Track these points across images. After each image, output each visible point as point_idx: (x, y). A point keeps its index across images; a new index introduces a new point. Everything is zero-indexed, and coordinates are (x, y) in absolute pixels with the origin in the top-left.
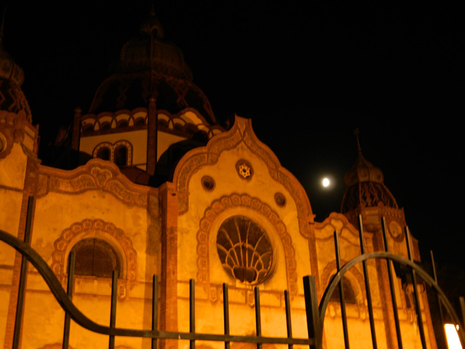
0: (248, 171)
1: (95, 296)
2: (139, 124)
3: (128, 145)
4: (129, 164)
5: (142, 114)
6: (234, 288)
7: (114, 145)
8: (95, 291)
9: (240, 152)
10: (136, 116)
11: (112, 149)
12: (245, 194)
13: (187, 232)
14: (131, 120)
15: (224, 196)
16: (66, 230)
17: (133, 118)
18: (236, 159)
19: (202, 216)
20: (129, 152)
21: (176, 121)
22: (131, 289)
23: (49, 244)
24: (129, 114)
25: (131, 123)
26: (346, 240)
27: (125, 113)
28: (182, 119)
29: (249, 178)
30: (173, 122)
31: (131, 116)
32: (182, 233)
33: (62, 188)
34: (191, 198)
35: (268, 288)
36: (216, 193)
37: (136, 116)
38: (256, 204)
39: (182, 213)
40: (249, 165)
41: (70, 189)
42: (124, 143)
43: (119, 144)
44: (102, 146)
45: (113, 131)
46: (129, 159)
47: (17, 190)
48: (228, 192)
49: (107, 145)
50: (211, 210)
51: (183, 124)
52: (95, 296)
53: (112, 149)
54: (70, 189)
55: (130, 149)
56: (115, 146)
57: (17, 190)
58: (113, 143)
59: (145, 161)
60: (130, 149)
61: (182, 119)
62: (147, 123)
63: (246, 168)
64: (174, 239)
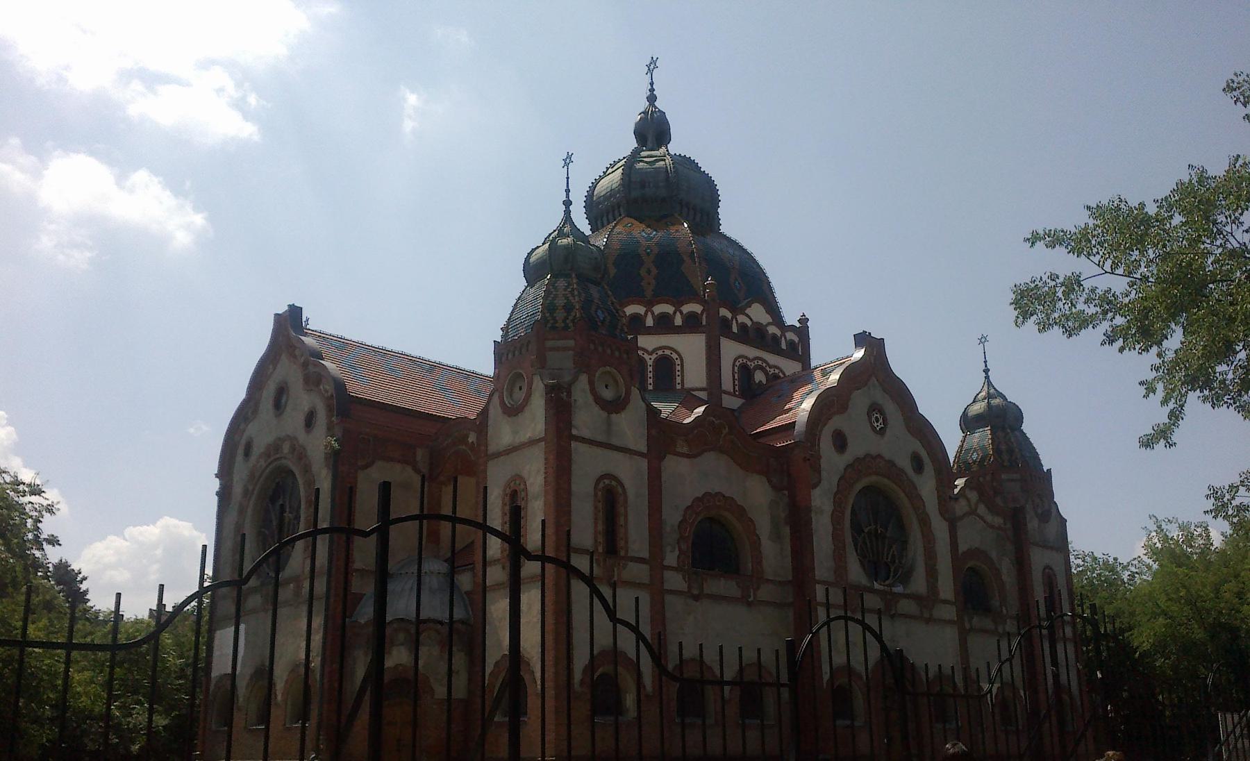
3: (675, 356)
4: (679, 387)
5: (697, 308)
6: (872, 590)
7: (651, 354)
10: (687, 308)
11: (650, 360)
12: (879, 456)
14: (678, 315)
15: (857, 460)
16: (688, 508)
17: (681, 313)
20: (679, 368)
22: (758, 588)
25: (678, 321)
26: (982, 518)
29: (882, 432)
31: (678, 310)
33: (679, 450)
34: (824, 464)
36: (848, 457)
37: (687, 308)
38: (891, 469)
39: (815, 486)
40: (881, 412)
41: (685, 450)
42: (667, 352)
43: (660, 352)
45: (649, 331)
46: (678, 380)
48: (861, 453)
50: (845, 481)
51: (749, 323)
53: (650, 360)
54: (685, 450)
55: (678, 362)
56: (654, 356)
58: (650, 349)
60: (678, 362)
64: (809, 522)
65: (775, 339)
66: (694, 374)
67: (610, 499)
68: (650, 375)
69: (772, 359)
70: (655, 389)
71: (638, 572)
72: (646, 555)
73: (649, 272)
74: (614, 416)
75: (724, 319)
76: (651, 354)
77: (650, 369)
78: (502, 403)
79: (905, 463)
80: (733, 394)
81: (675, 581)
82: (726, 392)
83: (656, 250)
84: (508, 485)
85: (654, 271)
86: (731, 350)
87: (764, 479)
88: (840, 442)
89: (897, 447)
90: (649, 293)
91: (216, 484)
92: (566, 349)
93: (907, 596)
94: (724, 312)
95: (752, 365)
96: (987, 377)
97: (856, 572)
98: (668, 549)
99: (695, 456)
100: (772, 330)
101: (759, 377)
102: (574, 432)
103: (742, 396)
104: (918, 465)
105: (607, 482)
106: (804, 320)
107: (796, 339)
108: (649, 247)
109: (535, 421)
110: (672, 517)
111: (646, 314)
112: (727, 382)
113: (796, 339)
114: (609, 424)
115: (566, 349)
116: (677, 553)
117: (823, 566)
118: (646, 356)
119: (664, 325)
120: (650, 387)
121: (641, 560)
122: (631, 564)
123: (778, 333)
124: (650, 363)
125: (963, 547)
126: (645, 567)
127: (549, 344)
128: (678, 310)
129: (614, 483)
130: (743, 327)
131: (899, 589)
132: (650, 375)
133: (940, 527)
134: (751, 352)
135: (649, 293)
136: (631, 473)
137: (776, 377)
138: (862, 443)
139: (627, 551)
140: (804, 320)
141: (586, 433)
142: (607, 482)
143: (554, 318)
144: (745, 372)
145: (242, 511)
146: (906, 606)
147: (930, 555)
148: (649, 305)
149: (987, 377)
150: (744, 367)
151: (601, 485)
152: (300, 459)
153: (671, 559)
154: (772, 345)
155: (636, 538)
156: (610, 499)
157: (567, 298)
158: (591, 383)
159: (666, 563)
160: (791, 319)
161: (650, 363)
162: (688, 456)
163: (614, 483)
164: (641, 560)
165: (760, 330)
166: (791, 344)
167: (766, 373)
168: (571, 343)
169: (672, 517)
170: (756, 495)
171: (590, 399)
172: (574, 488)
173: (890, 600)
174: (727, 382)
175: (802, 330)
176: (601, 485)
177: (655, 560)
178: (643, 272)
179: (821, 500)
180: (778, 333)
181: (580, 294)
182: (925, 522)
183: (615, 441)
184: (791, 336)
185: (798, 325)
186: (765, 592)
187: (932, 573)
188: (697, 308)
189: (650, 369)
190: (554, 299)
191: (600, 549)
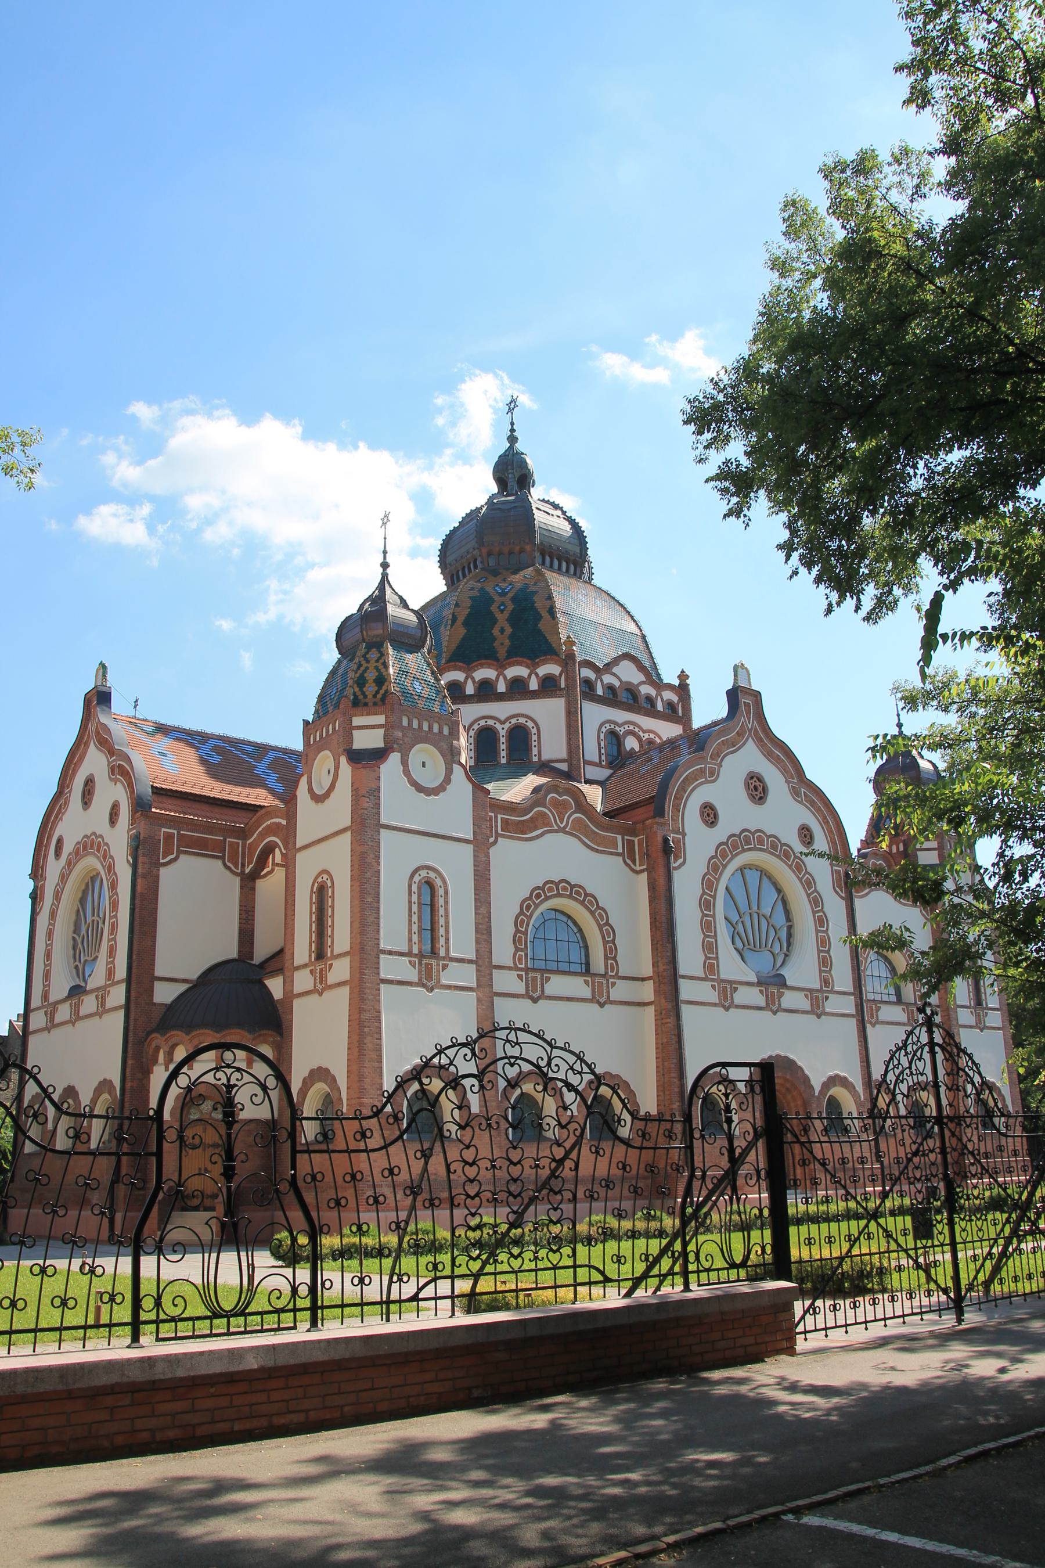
2: (549, 687)
3: (530, 724)
4: (535, 759)
5: (551, 669)
10: (543, 670)
11: (502, 730)
17: (537, 675)
20: (535, 737)
21: (608, 679)
24: (527, 667)
25: (534, 685)
27: (520, 664)
28: (614, 675)
30: (602, 681)
31: (533, 672)
37: (543, 670)
42: (522, 720)
43: (514, 721)
44: (482, 723)
45: (501, 697)
46: (535, 751)
49: (491, 722)
51: (617, 684)
53: (502, 730)
55: (534, 731)
56: (507, 726)
58: (502, 718)
59: (563, 754)
60: (534, 731)
61: (614, 675)
62: (563, 685)
63: (758, 783)
65: (649, 699)
66: (551, 745)
67: (428, 893)
68: (503, 747)
69: (646, 722)
70: (508, 763)
71: (468, 976)
73: (502, 631)
75: (588, 683)
76: (503, 723)
77: (503, 740)
80: (599, 765)
81: (507, 981)
82: (586, 762)
83: (511, 607)
85: (509, 630)
86: (595, 716)
88: (710, 815)
89: (782, 815)
90: (502, 652)
91: (30, 885)
92: (373, 727)
94: (587, 673)
95: (621, 730)
100: (646, 690)
101: (631, 744)
103: (610, 765)
104: (806, 834)
106: (683, 676)
107: (675, 698)
108: (503, 604)
109: (339, 809)
111: (498, 677)
112: (591, 747)
113: (675, 698)
115: (373, 727)
117: (689, 957)
118: (498, 726)
119: (518, 689)
120: (504, 761)
123: (653, 692)
124: (503, 733)
125: (864, 930)
127: (357, 721)
128: (533, 672)
129: (432, 875)
130: (611, 688)
132: (503, 747)
133: (834, 906)
134: (621, 716)
135: (502, 652)
137: (650, 742)
138: (738, 813)
139: (447, 950)
140: (683, 676)
143: (363, 693)
144: (615, 738)
145: (53, 915)
147: (823, 943)
148: (501, 667)
150: (613, 733)
152: (105, 858)
154: (647, 707)
155: (460, 938)
156: (428, 893)
157: (377, 668)
158: (405, 763)
160: (670, 677)
161: (503, 733)
165: (631, 690)
166: (670, 705)
167: (639, 739)
168: (380, 719)
170: (611, 880)
174: (591, 747)
175: (683, 689)
176: (417, 878)
178: (496, 631)
179: (686, 884)
180: (653, 692)
182: (816, 902)
184: (668, 695)
185: (677, 682)
186: (620, 990)
187: (825, 962)
188: (551, 669)
189: (503, 740)
190: (365, 671)
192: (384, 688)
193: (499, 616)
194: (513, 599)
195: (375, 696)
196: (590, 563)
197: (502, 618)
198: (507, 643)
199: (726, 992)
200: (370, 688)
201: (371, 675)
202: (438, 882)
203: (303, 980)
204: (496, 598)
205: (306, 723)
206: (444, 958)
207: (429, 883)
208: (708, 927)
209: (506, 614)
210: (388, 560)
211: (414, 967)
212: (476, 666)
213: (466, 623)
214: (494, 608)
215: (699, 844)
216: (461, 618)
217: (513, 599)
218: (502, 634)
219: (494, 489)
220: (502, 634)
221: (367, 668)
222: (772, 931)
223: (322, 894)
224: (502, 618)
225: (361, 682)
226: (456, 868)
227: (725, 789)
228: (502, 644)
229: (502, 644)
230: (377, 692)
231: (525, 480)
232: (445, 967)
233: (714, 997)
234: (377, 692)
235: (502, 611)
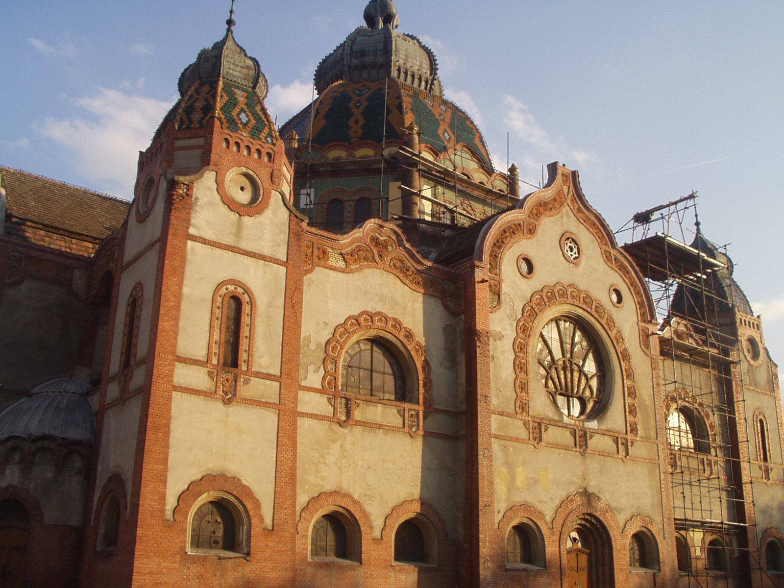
0: (575, 250)
1: (380, 426)
8: (379, 419)
9: (565, 219)
13: (501, 337)
18: (558, 232)
19: (519, 316)
23: (319, 345)
24: (374, 148)
32: (495, 340)
34: (505, 288)
35: (603, 427)
41: (341, 264)
47: (276, 261)
52: (380, 426)
57: (276, 261)
63: (572, 245)
72: (276, 371)
73: (356, 122)
74: (246, 220)
78: (138, 211)
79: (606, 299)
84: (131, 295)
85: (362, 121)
87: (440, 302)
92: (193, 148)
93: (604, 433)
96: (698, 230)
97: (540, 403)
98: (311, 368)
99: (351, 272)
102: (192, 231)
105: (231, 288)
106: (512, 170)
108: (359, 101)
110: (315, 330)
114: (239, 226)
115: (193, 148)
116: (322, 372)
121: (268, 377)
122: (253, 379)
126: (276, 385)
127: (179, 143)
129: (240, 290)
131: (593, 425)
136: (264, 284)
138: (552, 269)
140: (512, 170)
141: (209, 235)
142: (231, 288)
143: (191, 122)
146: (596, 442)
149: (698, 230)
151: (223, 291)
153: (314, 379)
157: (206, 100)
158: (220, 183)
159: (304, 383)
160: (500, 166)
162: (343, 271)
163: (240, 290)
164: (268, 377)
169: (315, 330)
171: (217, 198)
172: (186, 290)
173: (581, 439)
175: (511, 179)
177: (288, 375)
178: (351, 123)
181: (222, 97)
182: (625, 356)
183: (245, 245)
185: (506, 172)
190: (194, 102)
191: (215, 362)
192: (210, 115)
193: (355, 111)
194: (368, 99)
195: (200, 122)
196: (439, 82)
197: (357, 113)
198: (360, 131)
199: (537, 430)
200: (197, 116)
201: (200, 104)
202: (246, 298)
203: (113, 391)
204: (355, 98)
205: (141, 153)
206: (246, 373)
207: (236, 300)
208: (520, 367)
209: (362, 109)
210: (234, 17)
211: (212, 378)
212: (332, 146)
213: (327, 116)
214: (351, 105)
215: (516, 288)
216: (323, 113)
217: (368, 99)
218: (356, 124)
219: (364, 24)
220: (356, 124)
221: (198, 99)
222: (583, 378)
223: (134, 304)
224: (357, 113)
225: (189, 110)
226: (264, 284)
227: (543, 245)
228: (355, 132)
229: (355, 132)
230: (203, 119)
231: (389, 18)
232: (247, 382)
233: (523, 434)
234: (203, 119)
235: (358, 107)
